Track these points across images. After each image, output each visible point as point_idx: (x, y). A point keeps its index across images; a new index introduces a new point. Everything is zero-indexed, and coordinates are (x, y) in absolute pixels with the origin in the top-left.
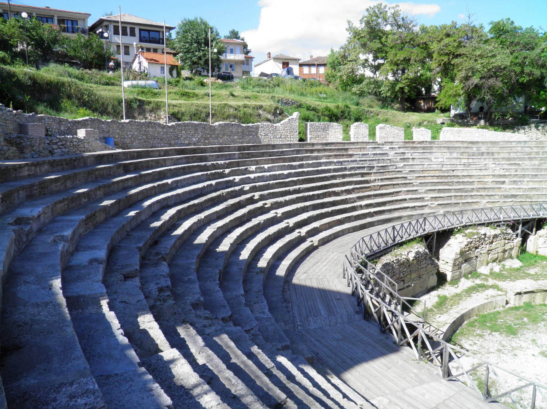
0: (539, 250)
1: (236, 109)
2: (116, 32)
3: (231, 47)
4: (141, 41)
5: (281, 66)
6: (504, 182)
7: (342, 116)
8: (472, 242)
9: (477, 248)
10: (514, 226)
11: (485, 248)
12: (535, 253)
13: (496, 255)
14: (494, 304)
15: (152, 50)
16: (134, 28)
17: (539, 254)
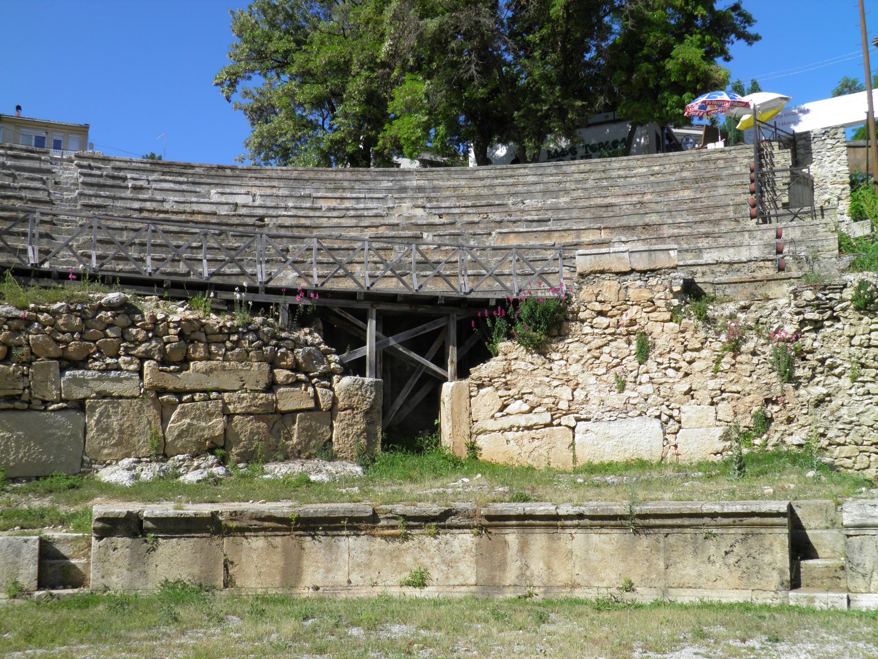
0: (481, 441)
3: (58, 136)
8: (28, 322)
9: (68, 363)
10: (336, 317)
12: (463, 453)
13: (218, 424)
17: (485, 455)
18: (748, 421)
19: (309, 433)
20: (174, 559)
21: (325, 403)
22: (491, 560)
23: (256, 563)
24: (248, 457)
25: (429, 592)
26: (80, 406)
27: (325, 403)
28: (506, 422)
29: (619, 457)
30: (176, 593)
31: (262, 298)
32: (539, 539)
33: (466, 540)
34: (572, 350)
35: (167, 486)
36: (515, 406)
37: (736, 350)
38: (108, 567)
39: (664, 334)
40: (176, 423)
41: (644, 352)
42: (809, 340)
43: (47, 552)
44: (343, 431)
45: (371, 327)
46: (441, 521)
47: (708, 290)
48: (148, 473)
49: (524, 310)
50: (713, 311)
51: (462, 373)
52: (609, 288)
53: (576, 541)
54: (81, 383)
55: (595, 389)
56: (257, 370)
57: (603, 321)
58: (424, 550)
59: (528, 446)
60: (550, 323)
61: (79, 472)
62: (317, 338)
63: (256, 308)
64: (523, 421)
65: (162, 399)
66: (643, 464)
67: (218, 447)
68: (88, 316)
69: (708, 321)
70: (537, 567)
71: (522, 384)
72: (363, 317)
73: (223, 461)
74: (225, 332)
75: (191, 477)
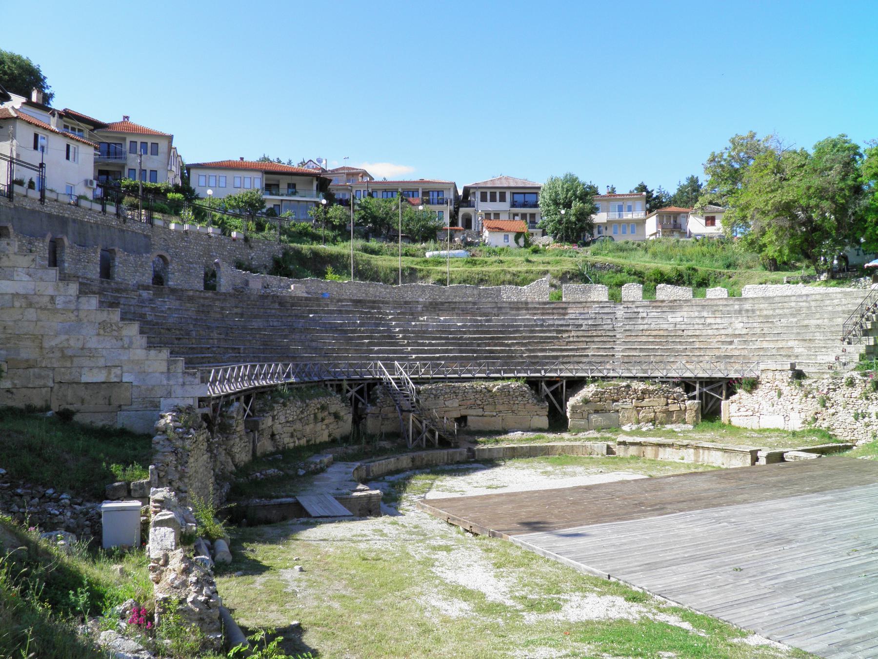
1: (514, 275)
2: (484, 199)
4: (514, 205)
5: (703, 221)
6: (731, 343)
7: (677, 280)
9: (614, 401)
10: (688, 385)
11: (629, 404)
12: (727, 423)
13: (652, 415)
14: (590, 451)
15: (492, 217)
16: (505, 193)
17: (733, 424)
18: (809, 419)
19: (678, 417)
20: (633, 451)
21: (683, 408)
22: (697, 455)
23: (649, 452)
24: (661, 423)
25: (685, 461)
26: (618, 411)
27: (683, 408)
28: (739, 414)
29: (772, 427)
30: (632, 457)
31: (664, 380)
32: (706, 452)
33: (692, 451)
34: (759, 392)
35: (638, 432)
36: (742, 409)
37: (806, 396)
38: (620, 451)
39: (786, 390)
40: (641, 415)
41: (780, 395)
42: (831, 395)
43: (608, 447)
44: (689, 416)
45: (698, 386)
46: (686, 446)
47: (807, 374)
48: (634, 427)
49: (743, 381)
50: (804, 382)
51: (727, 398)
52: (770, 375)
53: (713, 453)
54: (617, 406)
55: (766, 405)
56: (663, 400)
57: (768, 385)
58: (684, 452)
59: (746, 422)
60: (753, 385)
61: (616, 427)
62: (681, 390)
63: (663, 382)
64: (745, 414)
65: (638, 409)
66: (778, 430)
67: (653, 421)
68: (618, 389)
69: (801, 385)
70: (706, 458)
71: (744, 402)
72: (695, 382)
73: (654, 425)
74: (654, 391)
75: (644, 429)
